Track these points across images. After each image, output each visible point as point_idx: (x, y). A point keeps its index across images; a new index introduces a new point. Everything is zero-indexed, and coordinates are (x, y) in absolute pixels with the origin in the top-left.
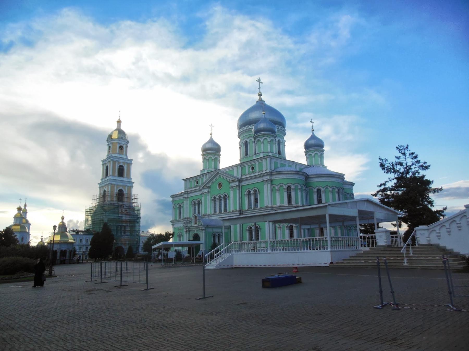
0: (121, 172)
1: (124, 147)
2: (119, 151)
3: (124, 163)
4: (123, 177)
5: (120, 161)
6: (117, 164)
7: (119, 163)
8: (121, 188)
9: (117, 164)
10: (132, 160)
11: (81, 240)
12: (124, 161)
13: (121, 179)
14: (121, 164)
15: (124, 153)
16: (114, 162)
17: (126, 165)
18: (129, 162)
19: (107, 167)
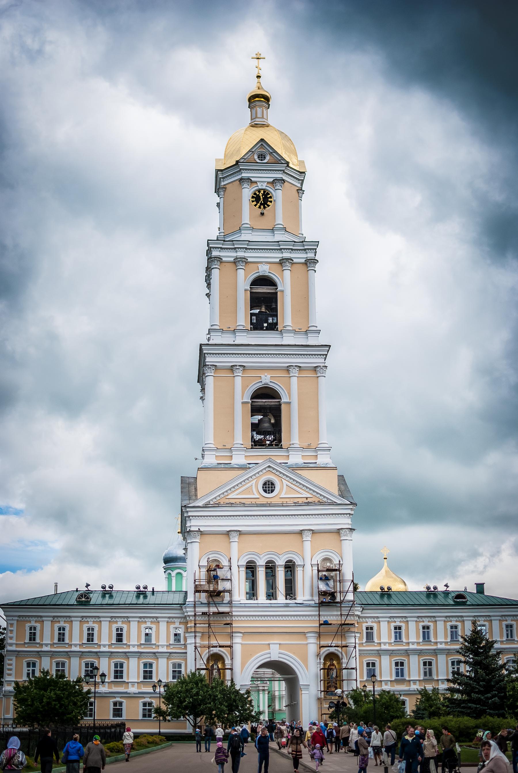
0: (264, 306)
6: (241, 273)
10: (314, 246)
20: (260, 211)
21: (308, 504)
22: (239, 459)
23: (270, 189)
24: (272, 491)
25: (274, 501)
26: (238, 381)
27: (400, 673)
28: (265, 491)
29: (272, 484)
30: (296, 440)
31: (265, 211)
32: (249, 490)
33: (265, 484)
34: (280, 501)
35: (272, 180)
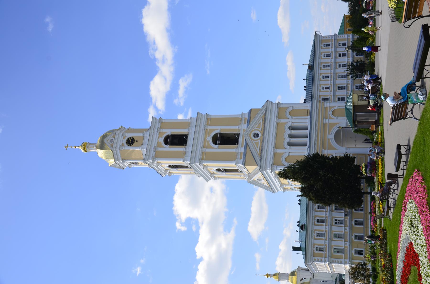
1: (129, 135)
2: (137, 146)
3: (160, 134)
4: (187, 136)
5: (154, 144)
6: (161, 149)
7: (159, 145)
8: (209, 139)
9: (161, 149)
11: (318, 235)
12: (156, 135)
13: (190, 140)
14: (162, 140)
15: (141, 135)
16: (158, 155)
17: (164, 131)
18: (158, 125)
19: (170, 166)
20: (135, 142)
21: (265, 118)
22: (242, 150)
23: (126, 138)
24: (258, 134)
25: (262, 133)
26: (208, 150)
27: (343, 88)
28: (258, 137)
29: (255, 134)
30: (237, 127)
31: (136, 139)
32: (257, 144)
33: (254, 137)
34: (263, 130)
35: (122, 137)
